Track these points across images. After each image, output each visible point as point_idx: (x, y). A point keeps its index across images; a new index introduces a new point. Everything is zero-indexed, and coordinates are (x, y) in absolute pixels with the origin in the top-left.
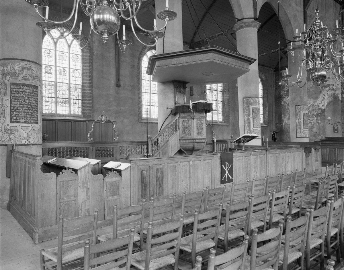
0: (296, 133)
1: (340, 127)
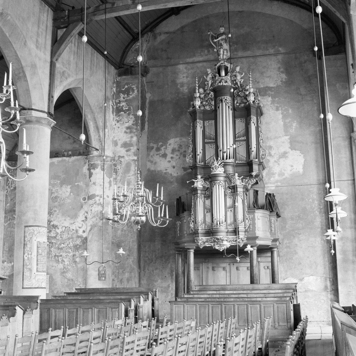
0: (23, 280)
1: (109, 272)
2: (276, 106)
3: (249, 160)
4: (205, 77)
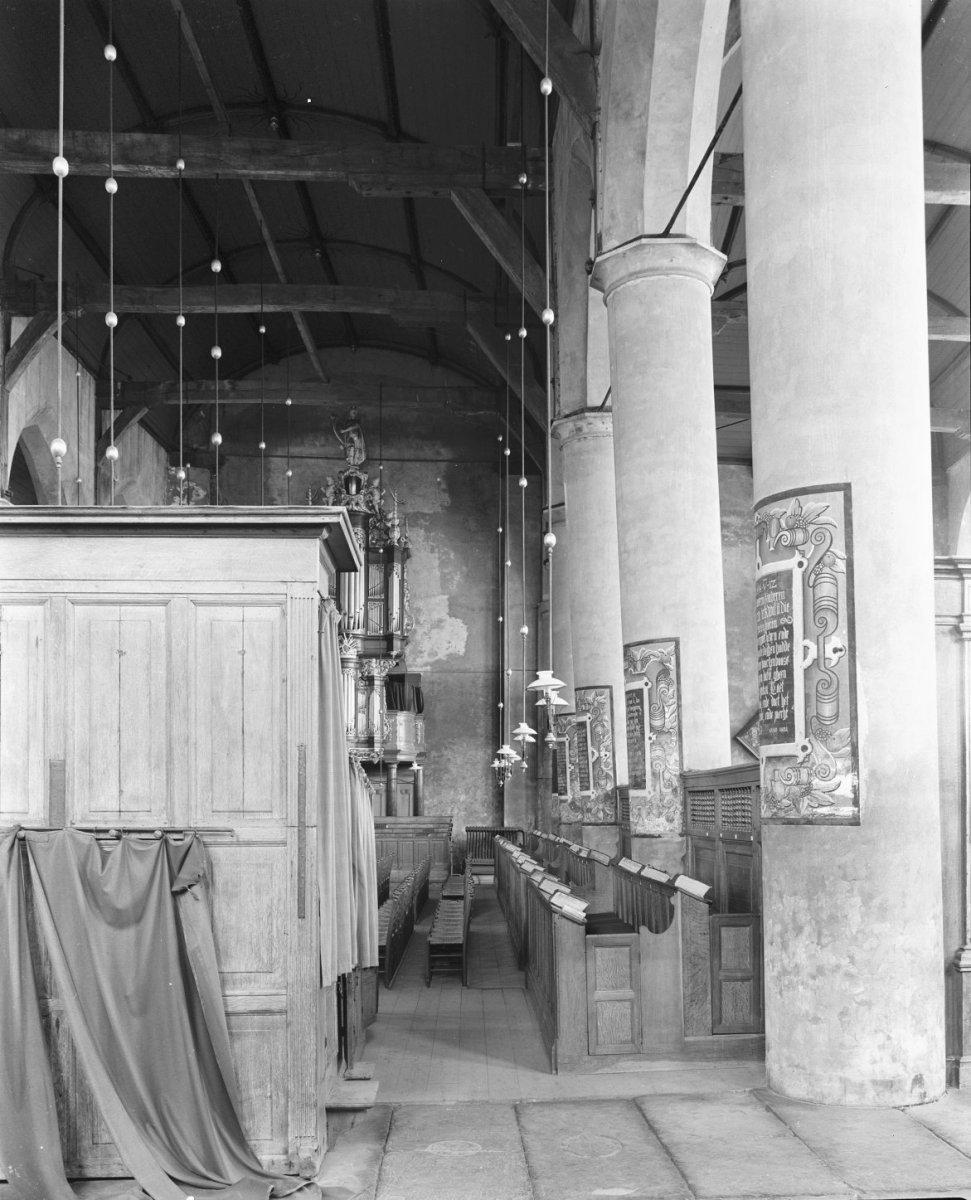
4: (322, 489)
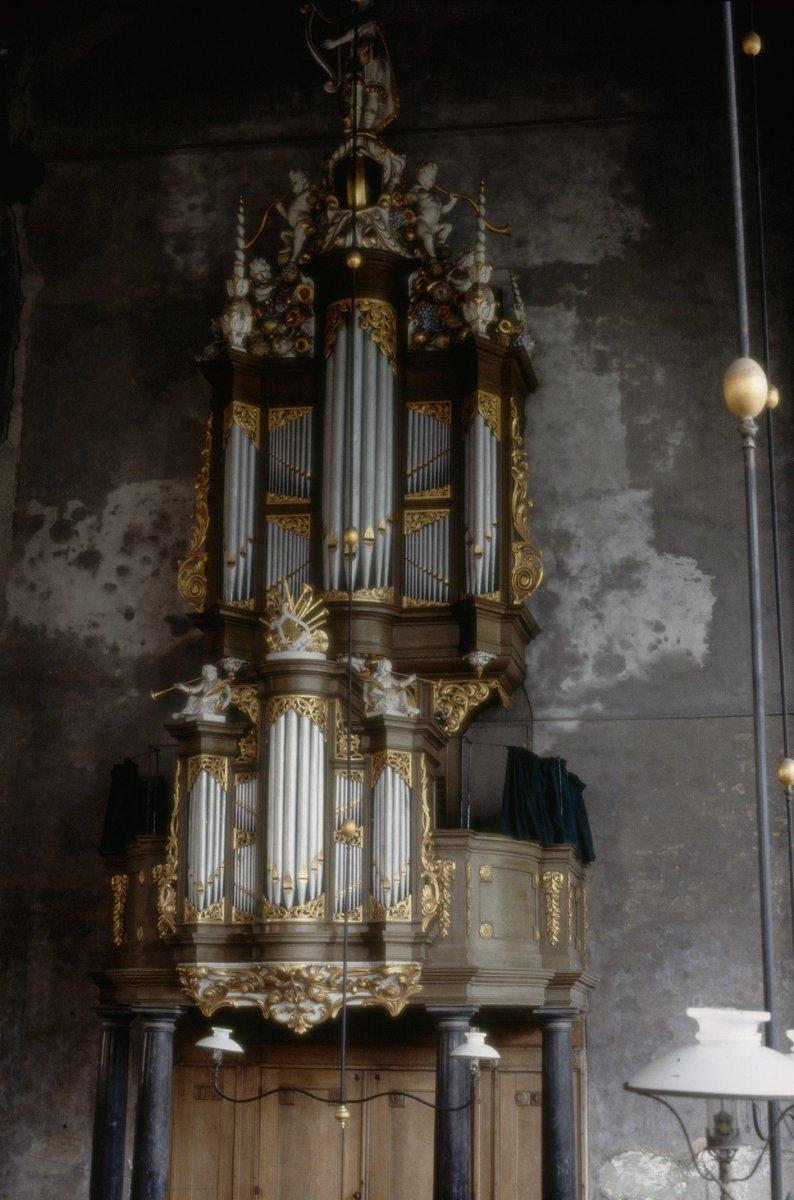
2: (597, 352)
3: (463, 597)
4: (280, 207)
